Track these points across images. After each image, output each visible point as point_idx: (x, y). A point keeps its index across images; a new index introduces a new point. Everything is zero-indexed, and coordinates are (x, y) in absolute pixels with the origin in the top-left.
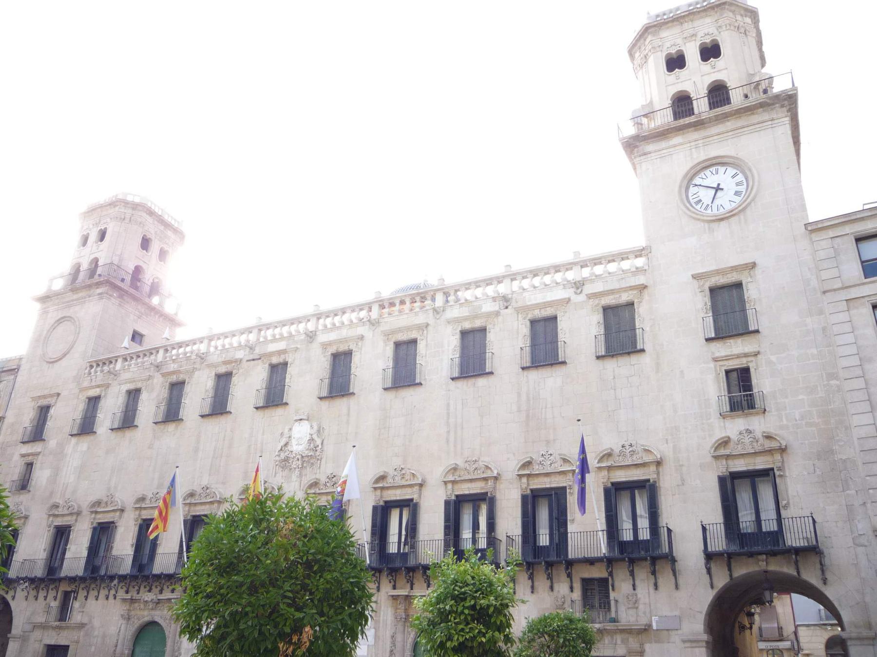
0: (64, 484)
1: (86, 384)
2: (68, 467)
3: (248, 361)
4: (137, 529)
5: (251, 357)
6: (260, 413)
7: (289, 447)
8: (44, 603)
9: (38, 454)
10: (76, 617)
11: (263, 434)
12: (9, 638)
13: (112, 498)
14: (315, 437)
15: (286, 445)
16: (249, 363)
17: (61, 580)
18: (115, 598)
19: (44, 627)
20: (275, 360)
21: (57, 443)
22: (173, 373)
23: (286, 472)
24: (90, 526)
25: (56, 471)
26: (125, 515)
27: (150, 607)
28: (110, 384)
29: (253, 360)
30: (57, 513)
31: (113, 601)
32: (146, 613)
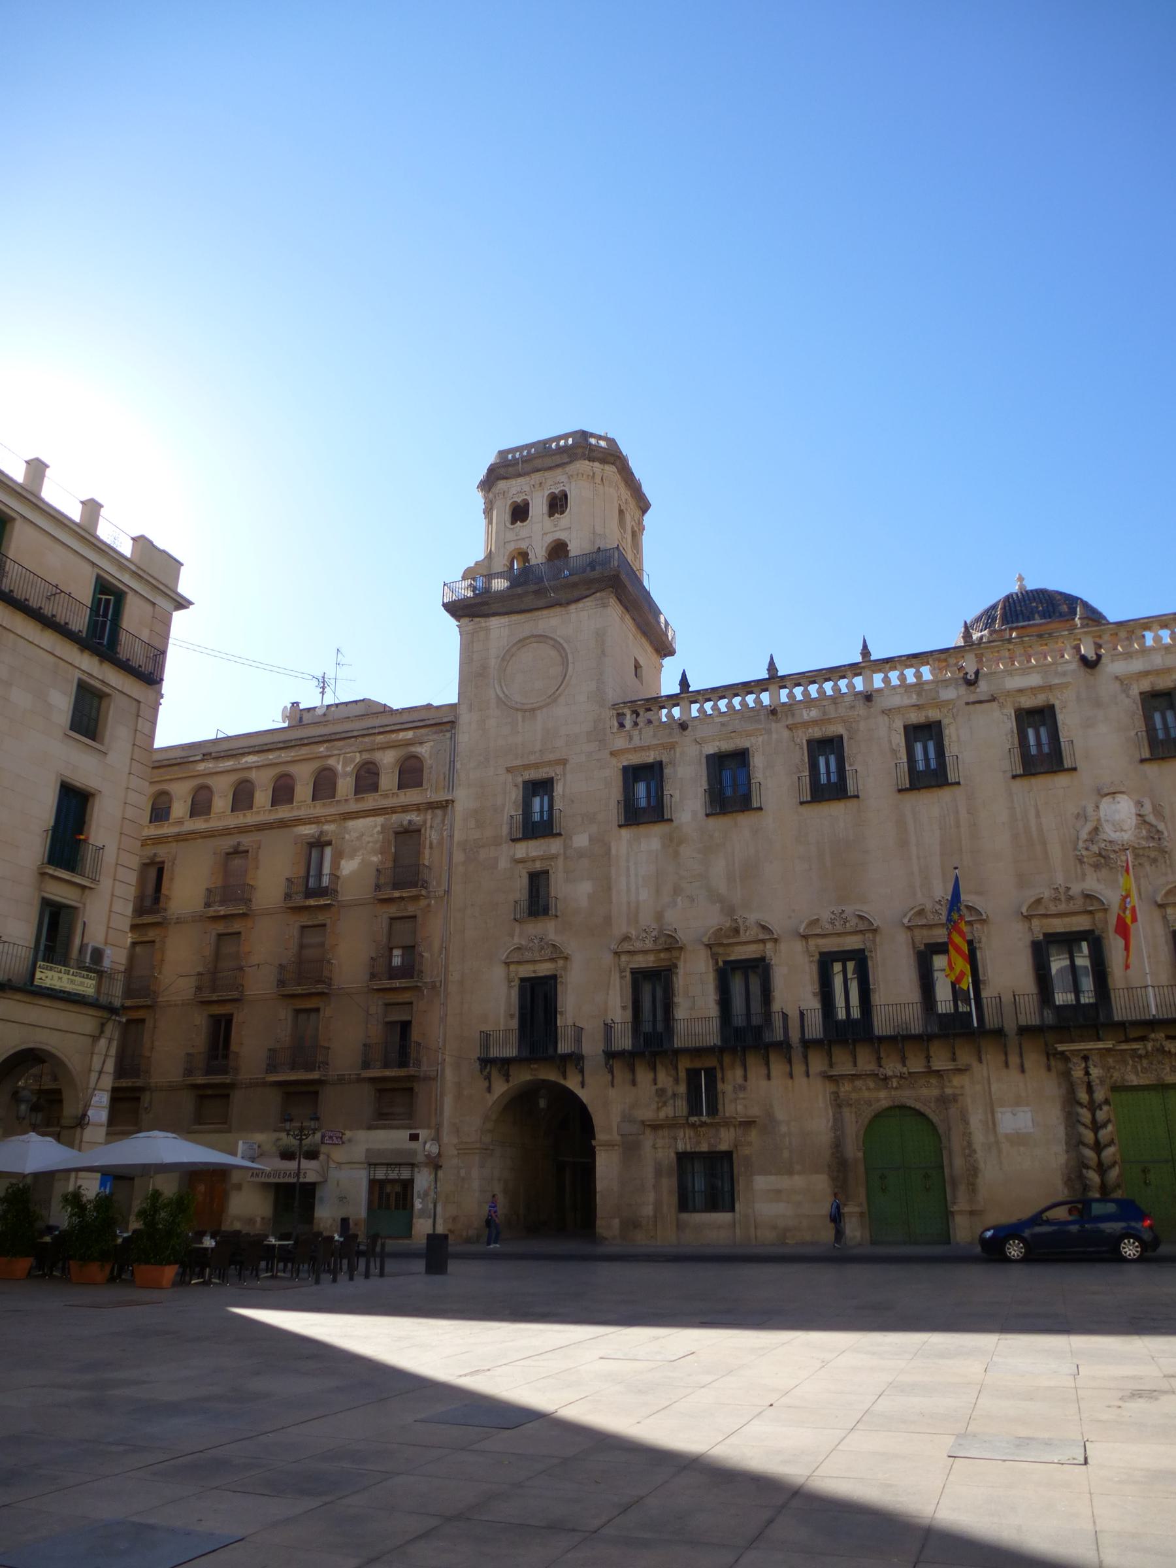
0: (629, 903)
1: (620, 743)
2: (628, 876)
3: (967, 704)
4: (814, 968)
5: (972, 698)
6: (1018, 782)
7: (1102, 836)
8: (654, 1088)
9: (554, 857)
10: (733, 1106)
11: (1038, 815)
12: (595, 1147)
13: (744, 922)
14: (1151, 818)
15: (1096, 830)
16: (971, 707)
17: (678, 1052)
18: (808, 1075)
19: (671, 1125)
20: (1027, 702)
21: (590, 840)
22: (815, 722)
23: (1104, 872)
24: (715, 968)
25: (605, 887)
26: (783, 947)
27: (895, 1085)
28: (676, 742)
29: (980, 702)
30: (631, 948)
31: (805, 1080)
32: (882, 1094)
